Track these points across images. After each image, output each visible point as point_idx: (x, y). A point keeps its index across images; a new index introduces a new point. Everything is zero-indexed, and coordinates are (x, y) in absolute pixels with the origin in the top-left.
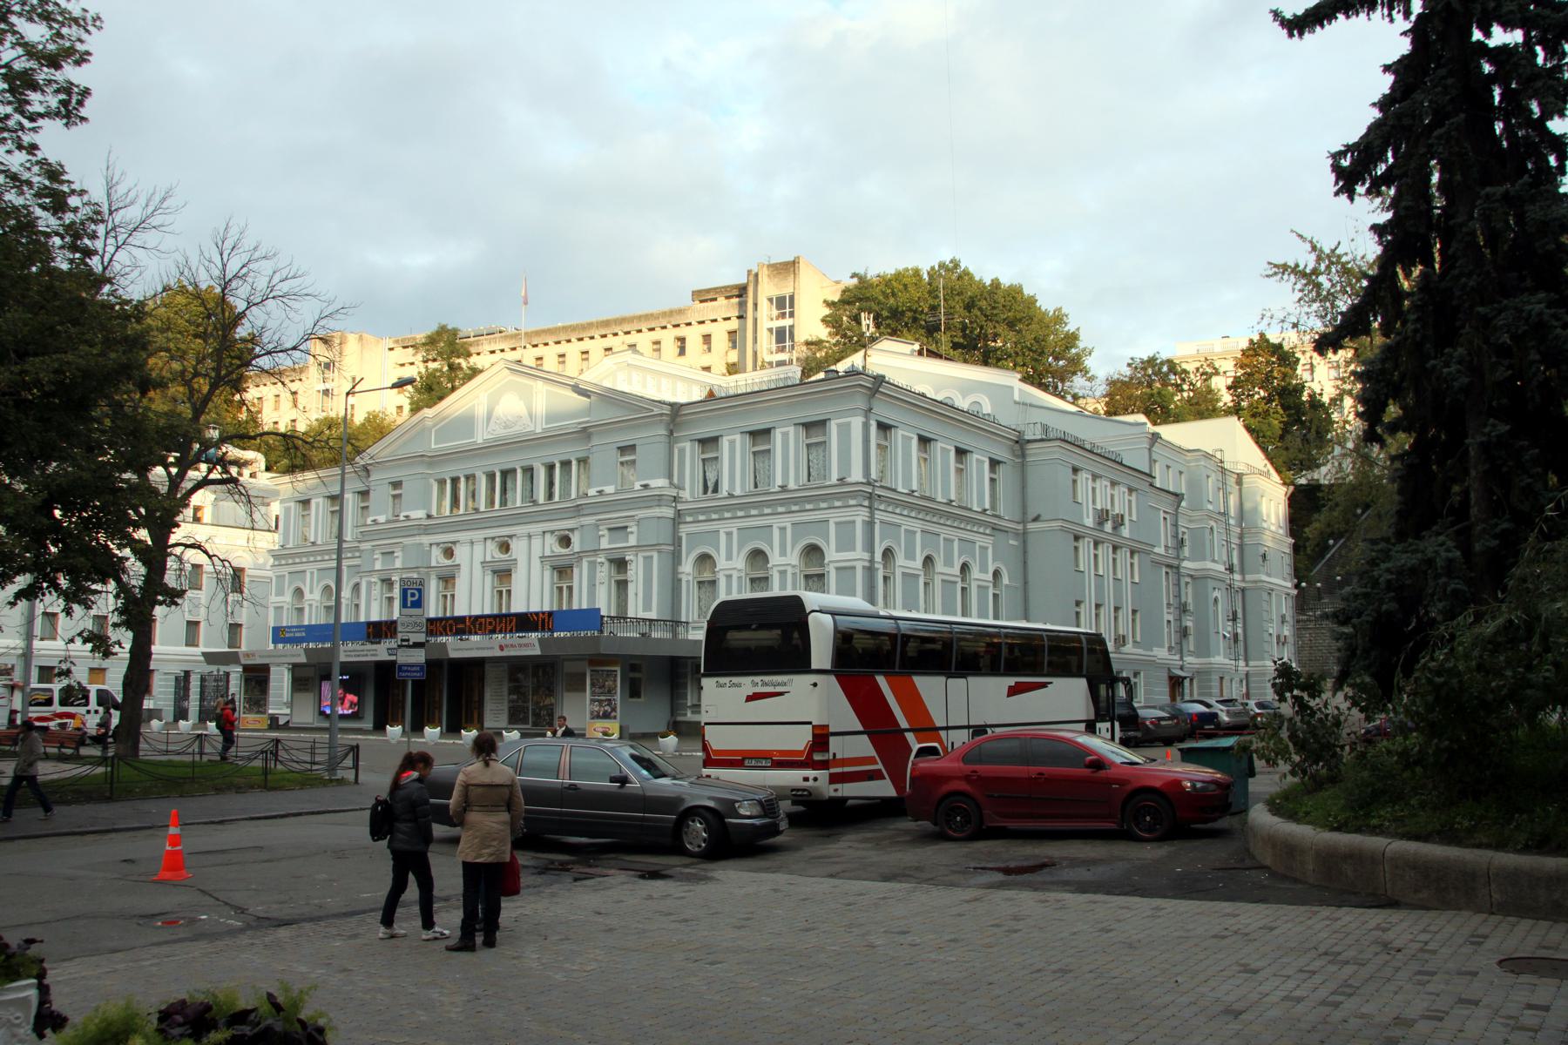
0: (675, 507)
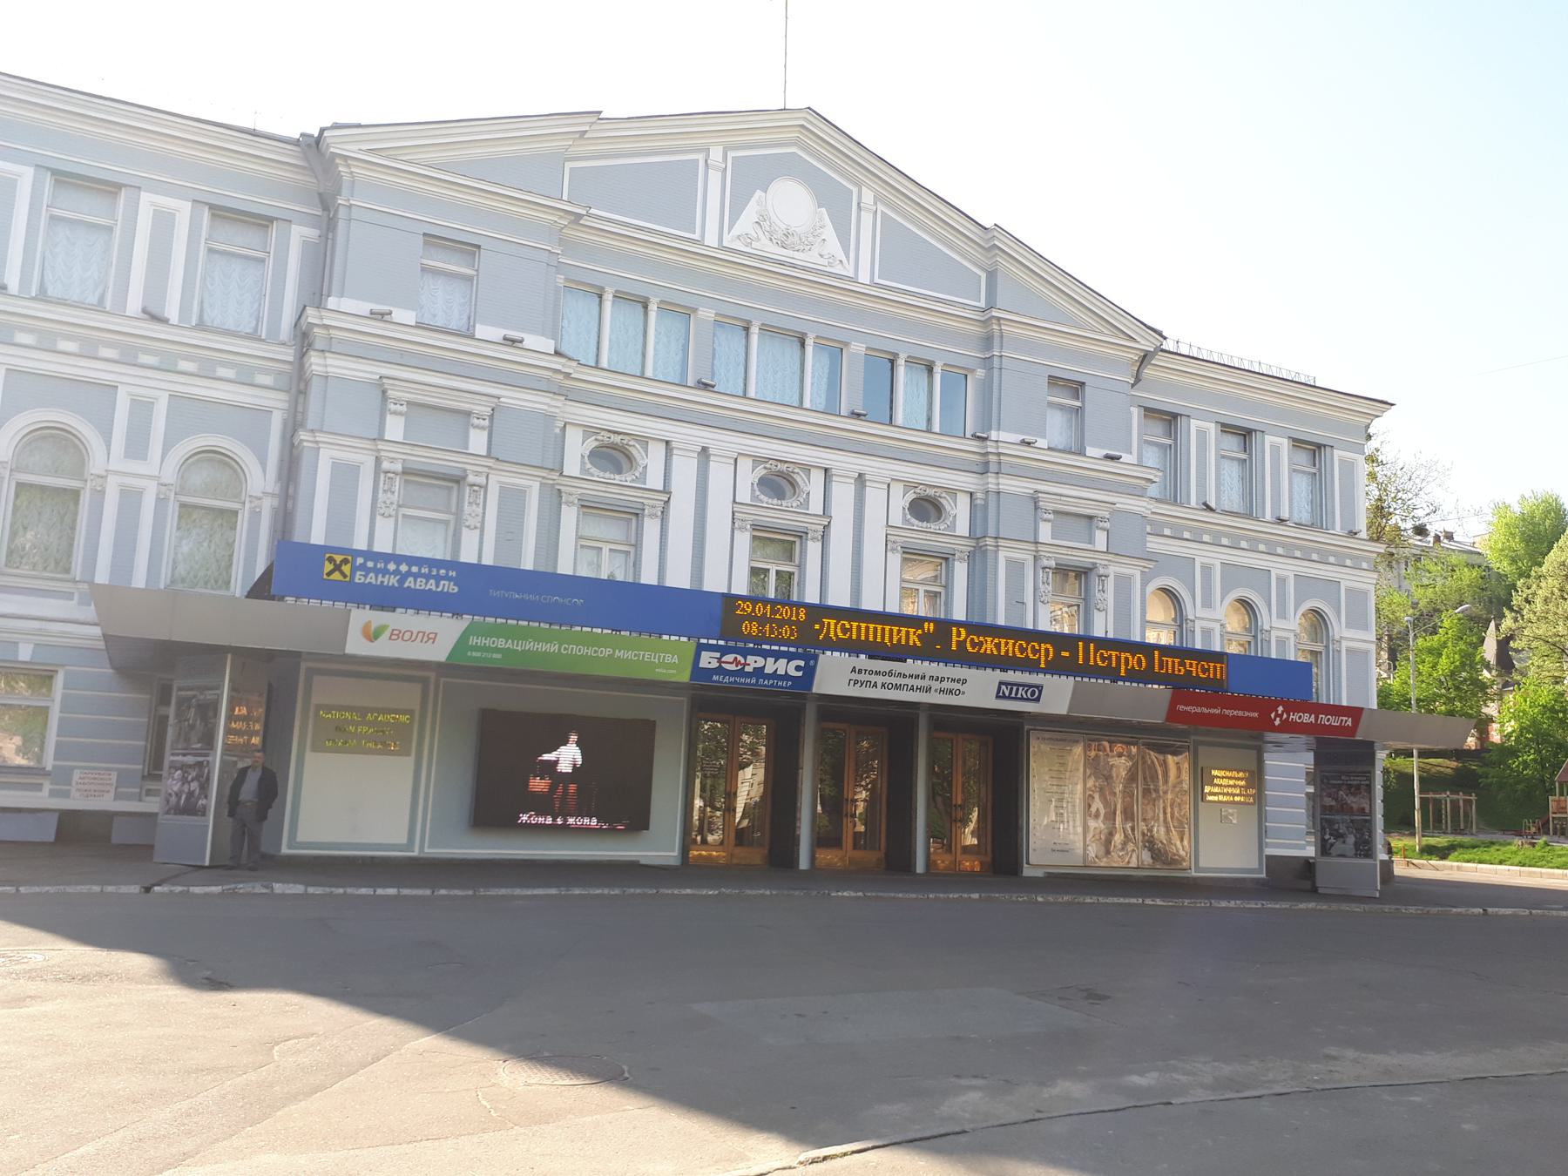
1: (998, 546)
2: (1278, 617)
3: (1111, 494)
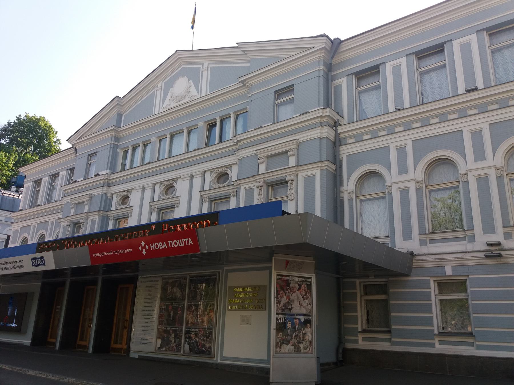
1: (239, 184)
2: (477, 159)
3: (296, 135)
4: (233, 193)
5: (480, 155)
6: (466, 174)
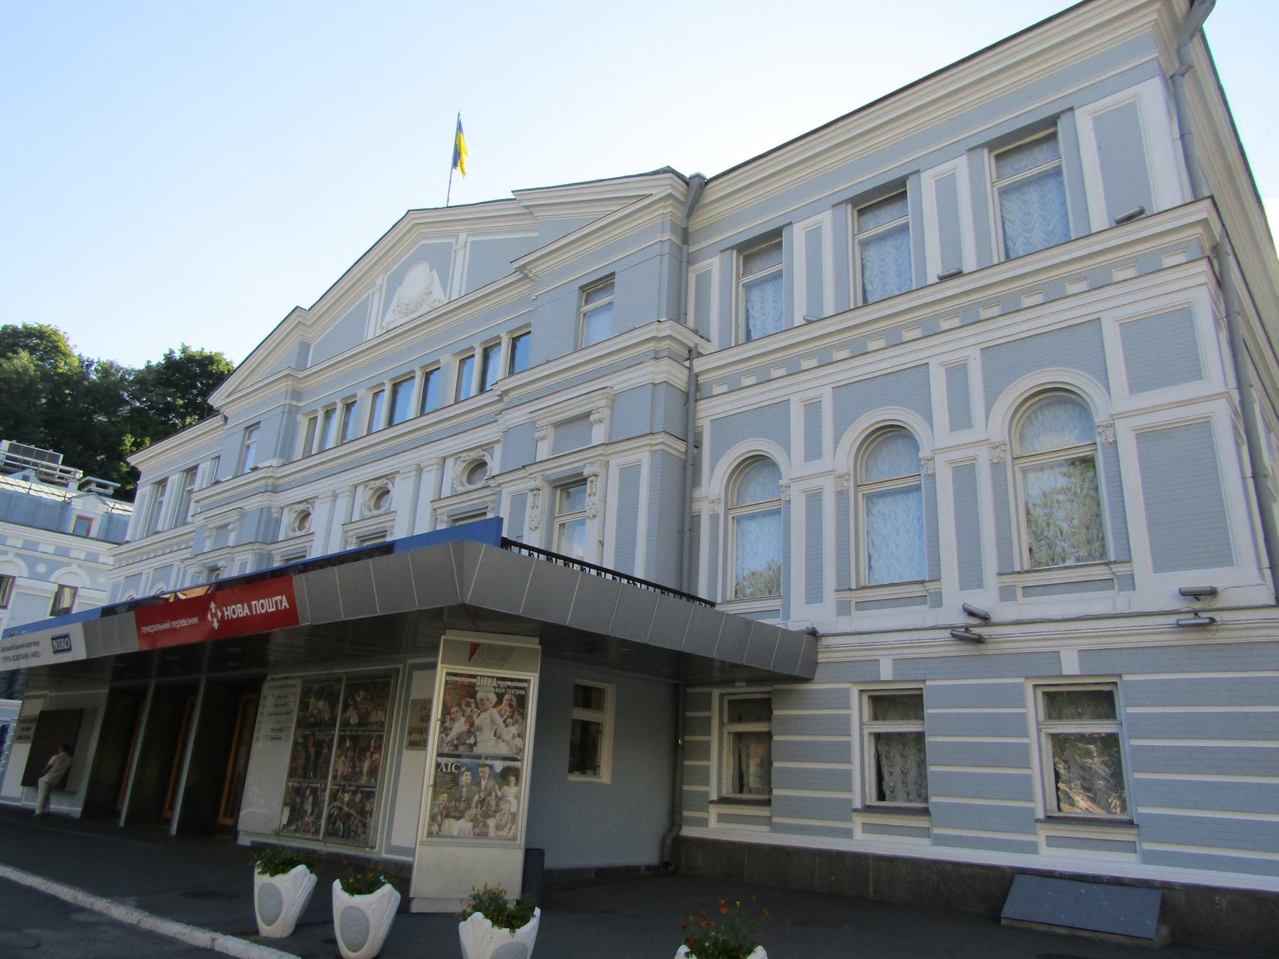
0: (690, 369)
4: (492, 505)
5: (960, 418)
6: (932, 459)
